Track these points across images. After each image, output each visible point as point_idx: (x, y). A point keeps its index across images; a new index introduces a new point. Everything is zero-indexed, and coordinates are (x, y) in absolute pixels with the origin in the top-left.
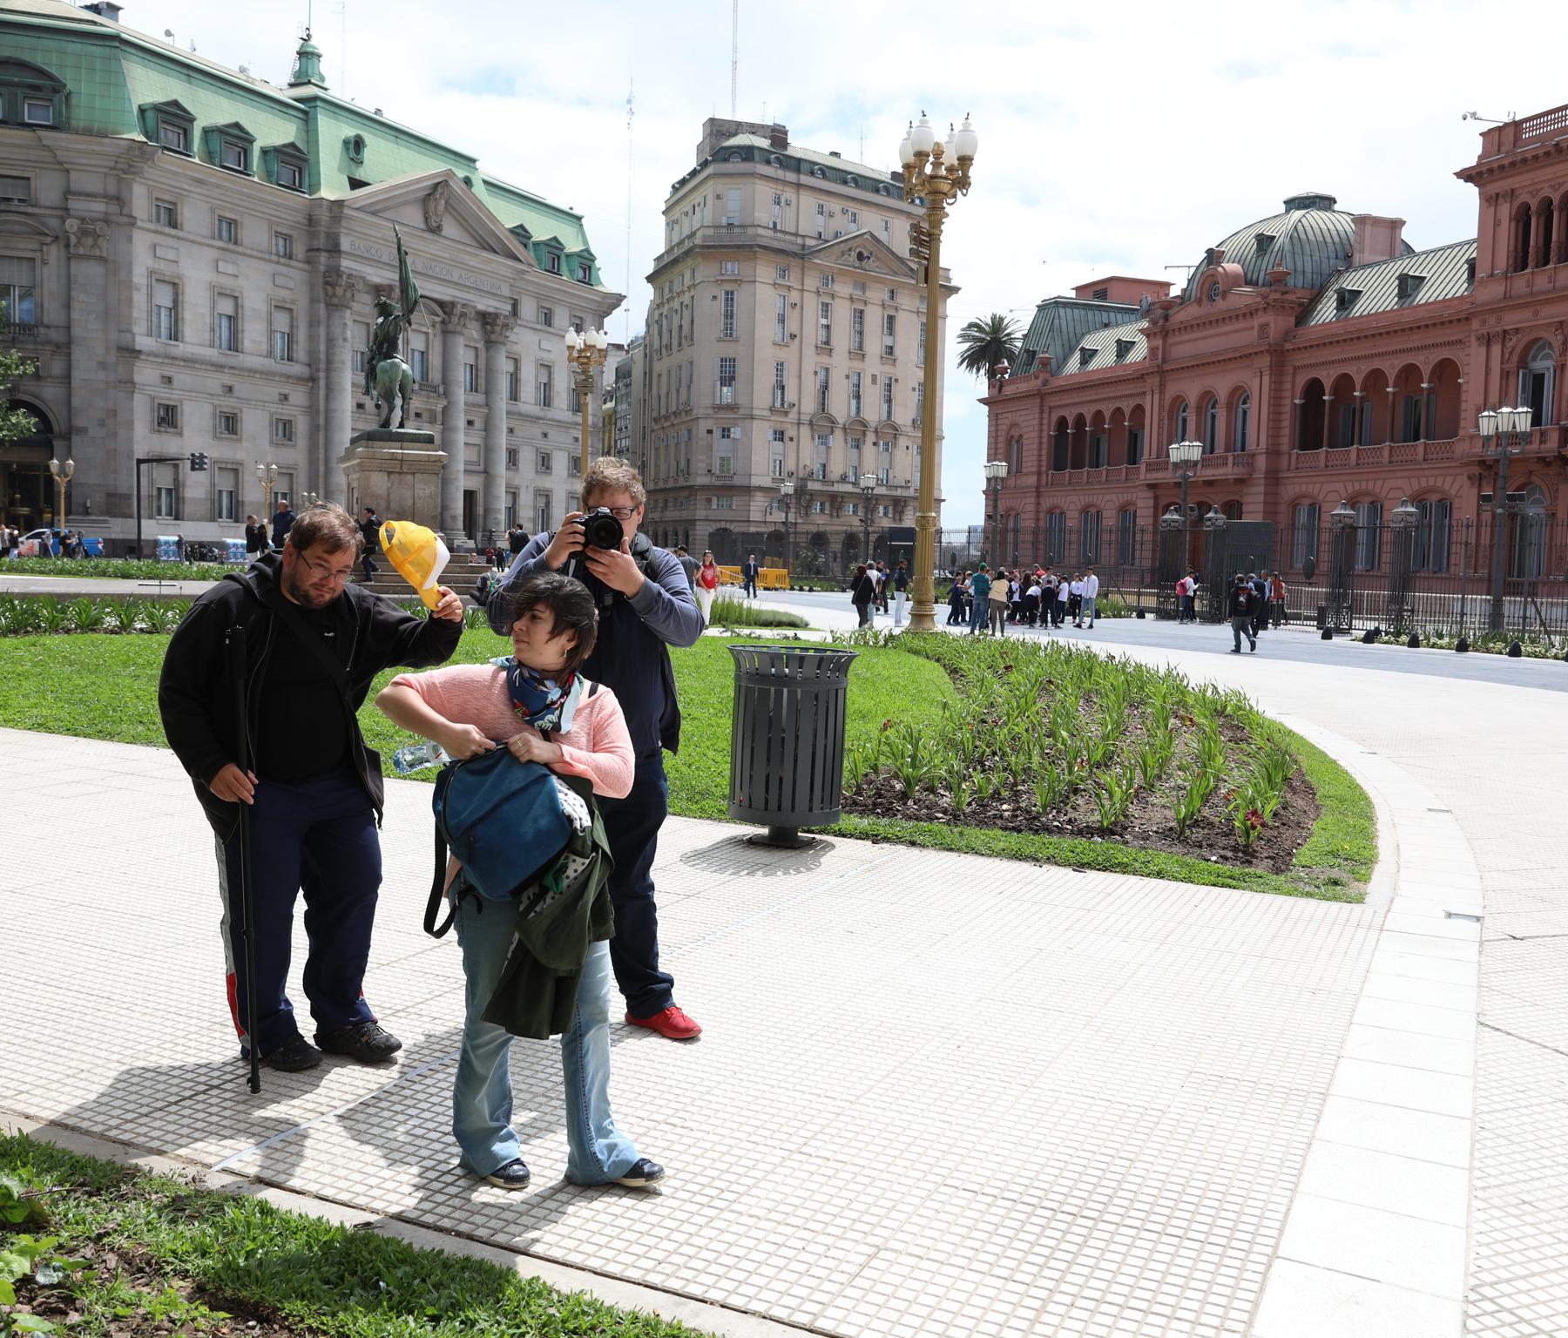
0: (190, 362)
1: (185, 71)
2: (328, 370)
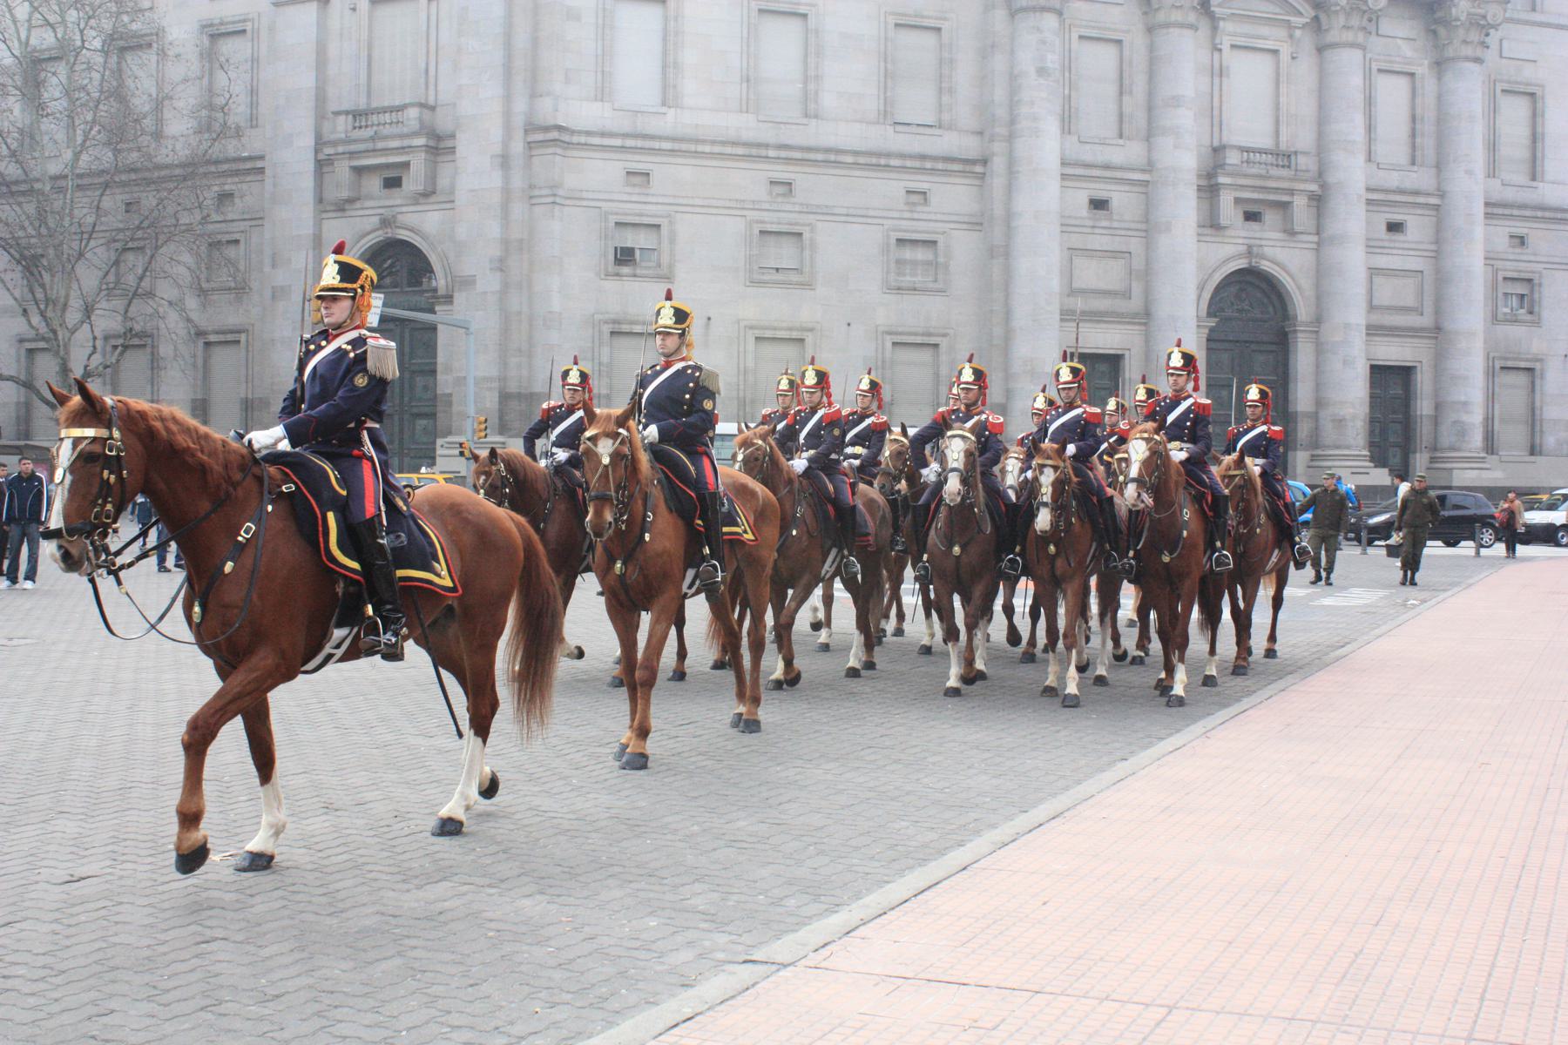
0: (684, 147)
2: (1011, 138)
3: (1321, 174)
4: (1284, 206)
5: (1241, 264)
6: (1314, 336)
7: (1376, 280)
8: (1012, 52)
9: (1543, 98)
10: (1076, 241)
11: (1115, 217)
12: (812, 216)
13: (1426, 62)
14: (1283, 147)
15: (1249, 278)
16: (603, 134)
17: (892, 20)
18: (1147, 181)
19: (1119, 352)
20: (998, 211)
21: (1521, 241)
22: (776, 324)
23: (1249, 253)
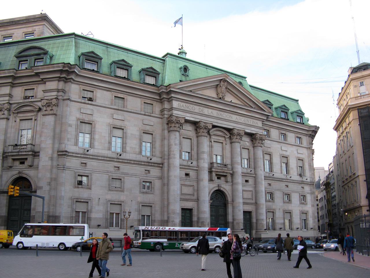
0: (95, 158)
1: (106, 46)
2: (169, 159)
3: (232, 169)
5: (217, 188)
6: (232, 205)
7: (244, 192)
8: (169, 140)
9: (272, 155)
10: (183, 183)
11: (190, 177)
12: (124, 175)
13: (251, 147)
14: (224, 163)
15: (218, 192)
16: (76, 154)
17: (142, 132)
18: (198, 170)
19: (192, 208)
20: (166, 175)
21: (270, 185)
22: (115, 200)
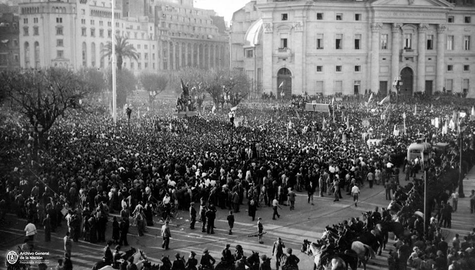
4: (412, 58)
23: (407, 65)
